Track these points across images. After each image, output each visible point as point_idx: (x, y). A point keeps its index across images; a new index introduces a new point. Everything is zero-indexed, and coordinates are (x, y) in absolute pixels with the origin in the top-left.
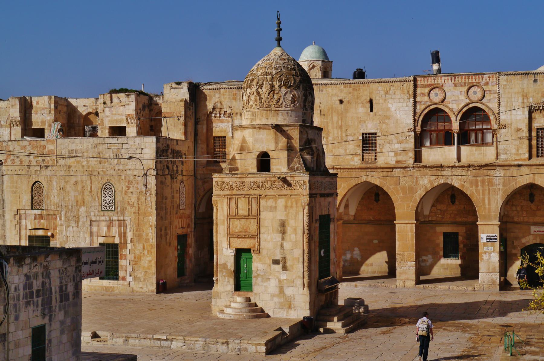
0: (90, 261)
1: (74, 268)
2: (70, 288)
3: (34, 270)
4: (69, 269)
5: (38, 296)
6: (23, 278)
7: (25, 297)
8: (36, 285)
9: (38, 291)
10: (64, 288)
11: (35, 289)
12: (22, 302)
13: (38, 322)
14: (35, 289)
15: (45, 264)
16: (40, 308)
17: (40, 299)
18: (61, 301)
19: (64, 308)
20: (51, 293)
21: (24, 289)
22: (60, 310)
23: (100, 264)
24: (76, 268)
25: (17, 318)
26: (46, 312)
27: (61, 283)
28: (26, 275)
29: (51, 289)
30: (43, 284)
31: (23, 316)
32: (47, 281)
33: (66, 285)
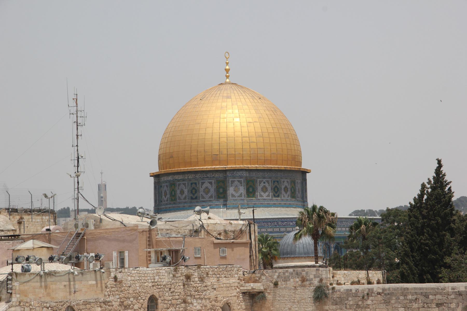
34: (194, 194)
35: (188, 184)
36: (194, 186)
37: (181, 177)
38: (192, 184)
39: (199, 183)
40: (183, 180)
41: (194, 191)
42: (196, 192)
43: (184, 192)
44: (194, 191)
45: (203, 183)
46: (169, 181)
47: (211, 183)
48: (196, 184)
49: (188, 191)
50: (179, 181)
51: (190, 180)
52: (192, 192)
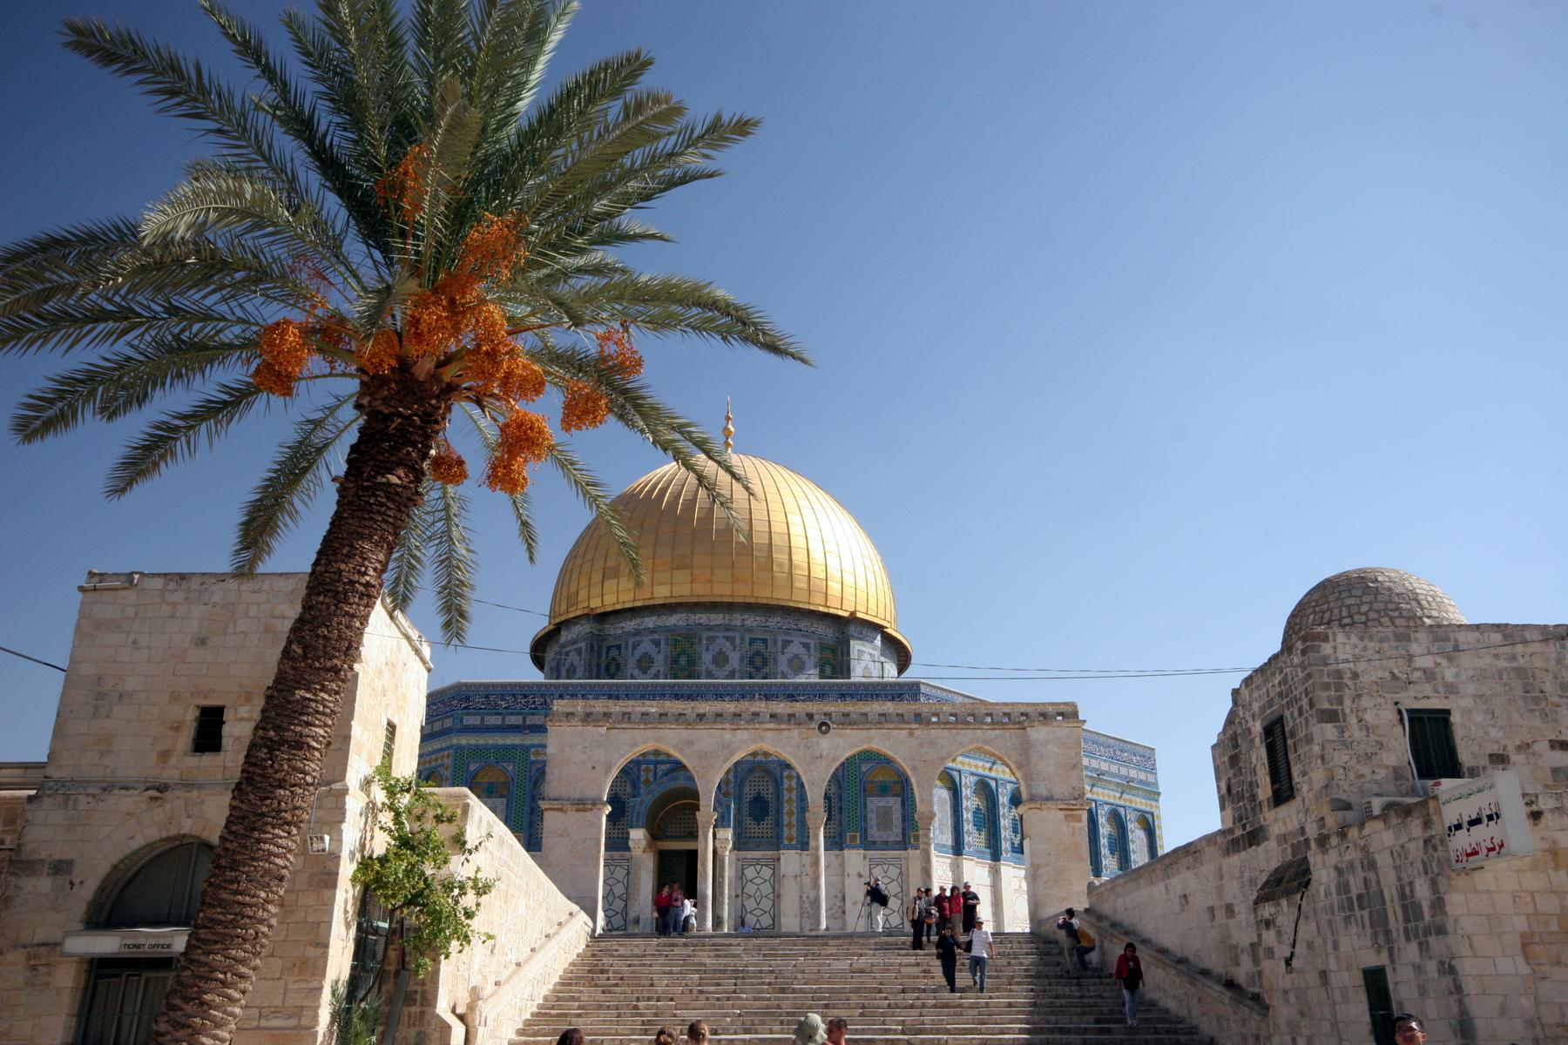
0: (1466, 819)
1: (1421, 843)
2: (1422, 891)
3: (1348, 857)
4: (1411, 846)
5: (1362, 907)
6: (1333, 873)
7: (1342, 908)
8: (1356, 886)
9: (1360, 897)
10: (1407, 890)
11: (1354, 893)
12: (1339, 918)
13: (1372, 960)
14: (1354, 893)
15: (1362, 842)
16: (1369, 932)
17: (1366, 913)
18: (1407, 920)
19: (1417, 936)
20: (1384, 902)
21: (1339, 893)
22: (1408, 939)
23: (1492, 823)
24: (1427, 842)
25: (1336, 946)
26: (1381, 940)
27: (1399, 879)
28: (1336, 868)
29: (1381, 892)
30: (1366, 881)
31: (1345, 945)
32: (1372, 876)
33: (1411, 884)
34: (758, 669)
35: (742, 639)
36: (759, 646)
37: (718, 619)
38: (752, 641)
39: (775, 642)
40: (727, 628)
41: (758, 660)
42: (765, 663)
43: (726, 660)
44: (758, 660)
45: (786, 643)
46: (669, 629)
47: (806, 646)
48: (765, 641)
49: (742, 660)
50: (710, 628)
51: (749, 630)
52: (751, 662)
